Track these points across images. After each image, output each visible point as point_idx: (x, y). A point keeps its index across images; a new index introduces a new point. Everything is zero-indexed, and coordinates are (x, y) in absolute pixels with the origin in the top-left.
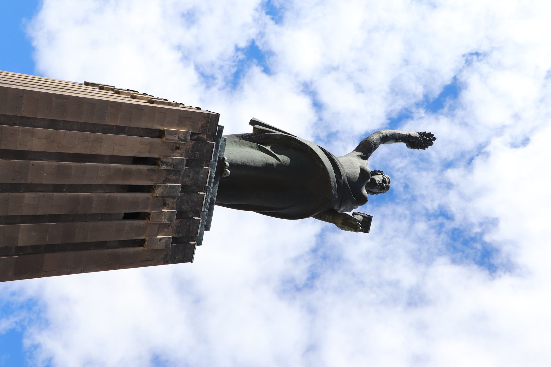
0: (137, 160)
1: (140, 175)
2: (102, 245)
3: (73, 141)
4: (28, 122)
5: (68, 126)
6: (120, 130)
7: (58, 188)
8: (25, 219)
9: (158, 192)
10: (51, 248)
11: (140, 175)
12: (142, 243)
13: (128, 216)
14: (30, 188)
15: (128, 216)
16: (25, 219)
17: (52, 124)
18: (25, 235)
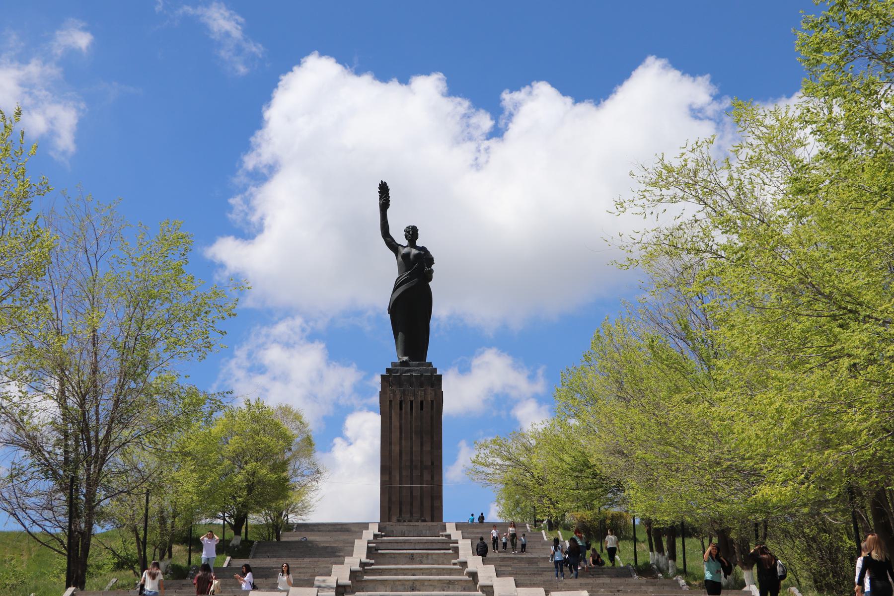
0: (401, 409)
1: (406, 407)
2: (432, 418)
3: (395, 435)
4: (390, 452)
5: (390, 438)
6: (390, 418)
7: (411, 439)
8: (422, 449)
9: (412, 399)
10: (432, 437)
11: (406, 407)
12: (432, 401)
13: (422, 409)
14: (411, 448)
15: (422, 409)
16: (422, 449)
17: (390, 444)
18: (427, 448)
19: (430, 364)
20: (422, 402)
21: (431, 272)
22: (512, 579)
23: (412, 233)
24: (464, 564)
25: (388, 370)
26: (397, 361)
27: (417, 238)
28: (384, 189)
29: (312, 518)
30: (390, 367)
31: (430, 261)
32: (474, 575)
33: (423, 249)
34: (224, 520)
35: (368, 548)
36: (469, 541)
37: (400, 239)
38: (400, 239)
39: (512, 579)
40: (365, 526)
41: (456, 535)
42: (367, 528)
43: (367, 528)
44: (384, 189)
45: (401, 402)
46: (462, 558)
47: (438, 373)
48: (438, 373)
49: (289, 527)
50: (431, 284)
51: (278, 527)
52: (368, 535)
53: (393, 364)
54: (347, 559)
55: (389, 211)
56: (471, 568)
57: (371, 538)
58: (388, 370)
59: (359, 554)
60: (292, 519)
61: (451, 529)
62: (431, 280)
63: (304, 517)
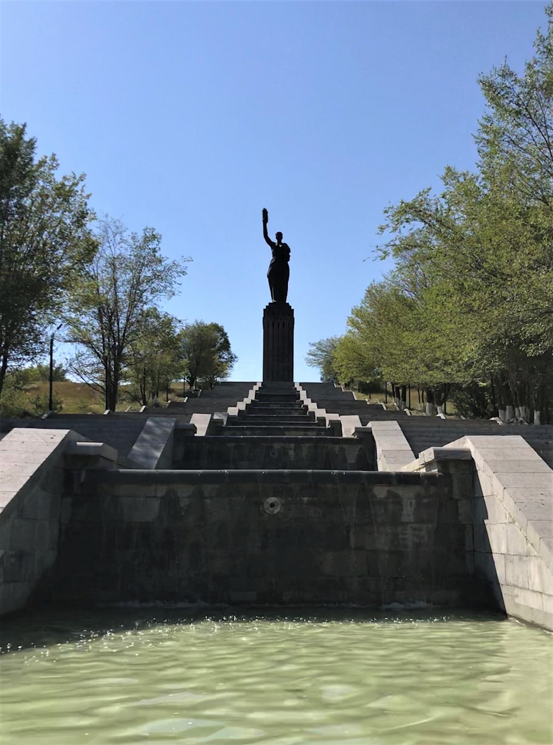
13: (284, 326)
15: (284, 326)
19: (288, 304)
20: (284, 323)
21: (289, 256)
22: (324, 410)
23: (279, 236)
24: (303, 401)
25: (267, 306)
26: (271, 302)
27: (282, 238)
28: (265, 212)
29: (229, 380)
30: (268, 305)
31: (289, 250)
32: (307, 407)
33: (285, 244)
34: (185, 379)
35: (256, 394)
36: (305, 391)
37: (274, 240)
38: (274, 240)
39: (324, 410)
40: (255, 383)
41: (299, 388)
42: (256, 385)
43: (256, 385)
44: (265, 212)
45: (273, 323)
46: (301, 399)
47: (292, 308)
48: (292, 308)
49: (217, 383)
50: (289, 263)
51: (212, 384)
52: (256, 388)
53: (270, 304)
54: (245, 399)
55: (268, 224)
56: (305, 404)
57: (258, 389)
58: (267, 306)
59: (252, 395)
60: (218, 379)
61: (297, 386)
62: (289, 260)
63: (224, 379)
